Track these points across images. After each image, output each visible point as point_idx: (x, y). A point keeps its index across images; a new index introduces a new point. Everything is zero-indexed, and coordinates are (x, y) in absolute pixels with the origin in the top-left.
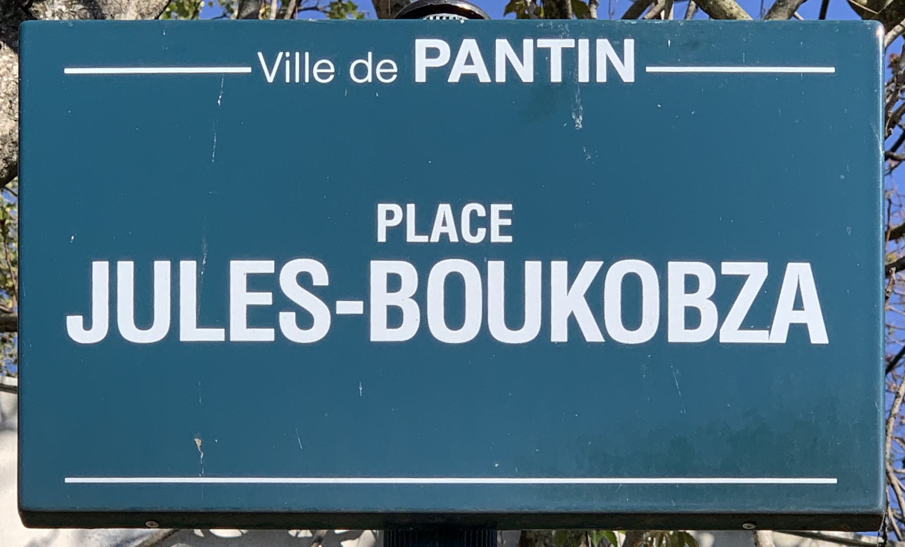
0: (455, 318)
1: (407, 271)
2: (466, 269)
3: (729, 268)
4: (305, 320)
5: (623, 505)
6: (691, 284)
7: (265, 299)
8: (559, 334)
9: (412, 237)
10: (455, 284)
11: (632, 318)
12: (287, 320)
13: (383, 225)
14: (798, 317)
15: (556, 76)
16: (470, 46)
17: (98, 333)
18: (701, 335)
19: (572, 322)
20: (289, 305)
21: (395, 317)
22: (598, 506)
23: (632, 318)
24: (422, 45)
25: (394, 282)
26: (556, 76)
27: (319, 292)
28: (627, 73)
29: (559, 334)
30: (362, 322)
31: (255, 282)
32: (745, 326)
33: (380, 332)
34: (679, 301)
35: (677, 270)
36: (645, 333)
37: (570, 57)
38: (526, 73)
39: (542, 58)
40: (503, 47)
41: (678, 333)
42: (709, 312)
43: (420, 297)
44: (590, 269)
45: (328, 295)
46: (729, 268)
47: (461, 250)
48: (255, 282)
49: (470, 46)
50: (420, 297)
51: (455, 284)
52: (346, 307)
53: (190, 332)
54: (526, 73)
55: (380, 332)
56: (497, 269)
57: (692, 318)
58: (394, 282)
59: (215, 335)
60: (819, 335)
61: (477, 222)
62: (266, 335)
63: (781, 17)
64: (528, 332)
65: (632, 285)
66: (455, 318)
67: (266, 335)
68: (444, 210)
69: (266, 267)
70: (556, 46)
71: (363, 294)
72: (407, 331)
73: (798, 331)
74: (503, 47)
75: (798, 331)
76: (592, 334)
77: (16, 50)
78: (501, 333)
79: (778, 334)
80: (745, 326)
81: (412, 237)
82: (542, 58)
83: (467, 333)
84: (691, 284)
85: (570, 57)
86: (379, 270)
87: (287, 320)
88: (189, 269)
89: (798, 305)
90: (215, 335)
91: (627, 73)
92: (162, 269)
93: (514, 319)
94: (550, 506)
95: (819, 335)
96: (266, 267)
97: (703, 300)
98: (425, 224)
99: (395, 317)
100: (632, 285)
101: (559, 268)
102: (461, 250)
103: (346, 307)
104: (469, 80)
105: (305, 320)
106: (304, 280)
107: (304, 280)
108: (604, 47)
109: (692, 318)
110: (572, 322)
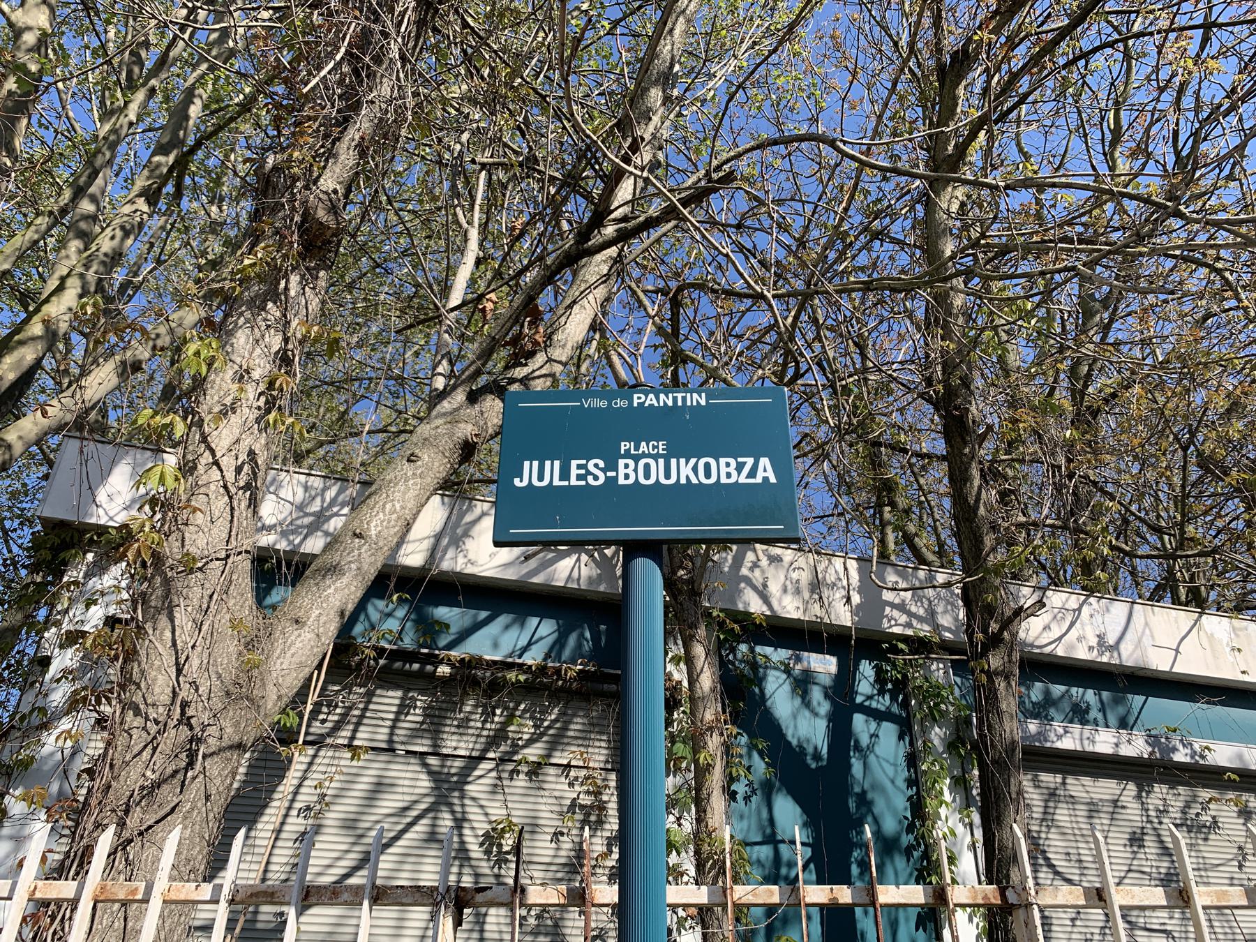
0: (647, 476)
1: (631, 463)
2: (651, 462)
3: (740, 460)
4: (596, 478)
5: (708, 536)
6: (728, 465)
7: (583, 472)
8: (683, 481)
9: (632, 452)
10: (647, 466)
11: (708, 475)
12: (590, 478)
13: (623, 448)
14: (765, 475)
15: (680, 403)
16: (651, 396)
17: (525, 483)
18: (732, 480)
19: (687, 477)
20: (591, 474)
21: (627, 477)
22: (698, 536)
23: (708, 475)
24: (635, 396)
25: (626, 466)
26: (680, 403)
27: (601, 469)
28: (703, 402)
29: (683, 481)
30: (616, 477)
31: (579, 467)
32: (747, 477)
33: (621, 481)
34: (724, 470)
35: (723, 461)
36: (713, 480)
37: (684, 399)
38: (670, 403)
39: (675, 399)
40: (662, 396)
41: (724, 480)
42: (734, 474)
43: (636, 470)
44: (693, 461)
45: (604, 470)
46: (740, 460)
47: (649, 456)
48: (579, 467)
49: (651, 396)
50: (636, 470)
51: (647, 466)
52: (609, 474)
53: (556, 482)
54: (670, 403)
55: (621, 481)
56: (661, 461)
57: (729, 475)
58: (626, 466)
59: (566, 483)
60: (773, 480)
61: (654, 447)
62: (583, 483)
63: (750, 385)
64: (673, 480)
65: (707, 466)
66: (647, 476)
67: (583, 483)
68: (643, 444)
69: (584, 462)
70: (679, 396)
71: (616, 470)
72: (631, 481)
73: (766, 479)
74: (662, 396)
75: (766, 479)
76: (694, 481)
77: (503, 401)
78: (663, 481)
79: (759, 480)
80: (747, 477)
81: (632, 452)
82: (675, 399)
83: (652, 481)
84: (728, 465)
85: (684, 399)
86: (621, 462)
87: (590, 478)
88: (557, 463)
89: (765, 470)
90: (566, 483)
91: (703, 402)
92: (548, 463)
93: (668, 476)
94: (681, 537)
95: (773, 480)
96: (584, 462)
97: (732, 469)
98: (637, 448)
99: (627, 477)
100: (707, 466)
101: (682, 461)
102: (649, 456)
103: (609, 474)
104: (651, 406)
105: (596, 478)
106: (596, 466)
107: (596, 466)
108: (695, 395)
109: (729, 475)
110: (687, 477)
